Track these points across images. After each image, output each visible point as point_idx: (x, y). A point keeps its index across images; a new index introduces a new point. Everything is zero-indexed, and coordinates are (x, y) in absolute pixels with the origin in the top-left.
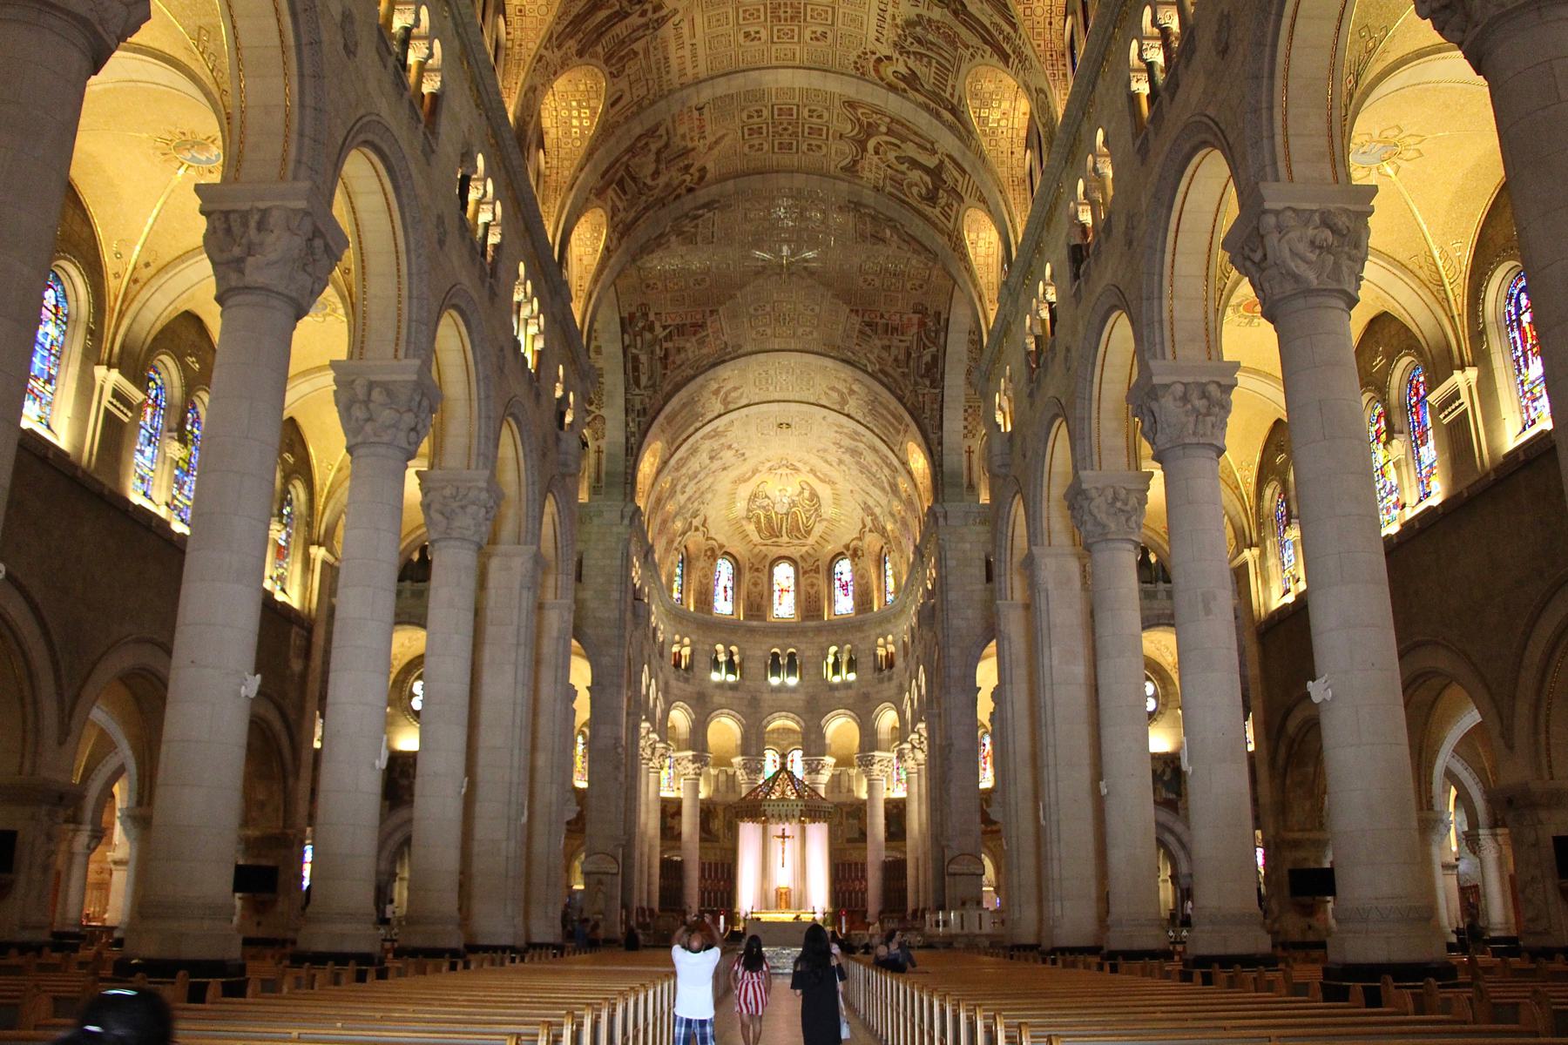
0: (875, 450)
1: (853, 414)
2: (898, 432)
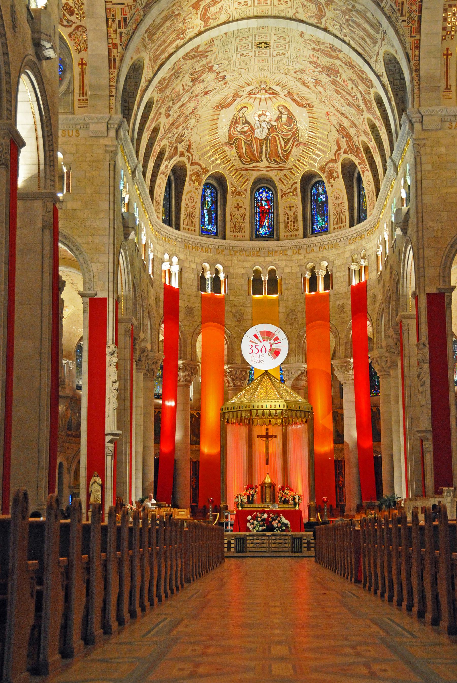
0: (351, 66)
1: (330, 28)
2: (375, 43)
